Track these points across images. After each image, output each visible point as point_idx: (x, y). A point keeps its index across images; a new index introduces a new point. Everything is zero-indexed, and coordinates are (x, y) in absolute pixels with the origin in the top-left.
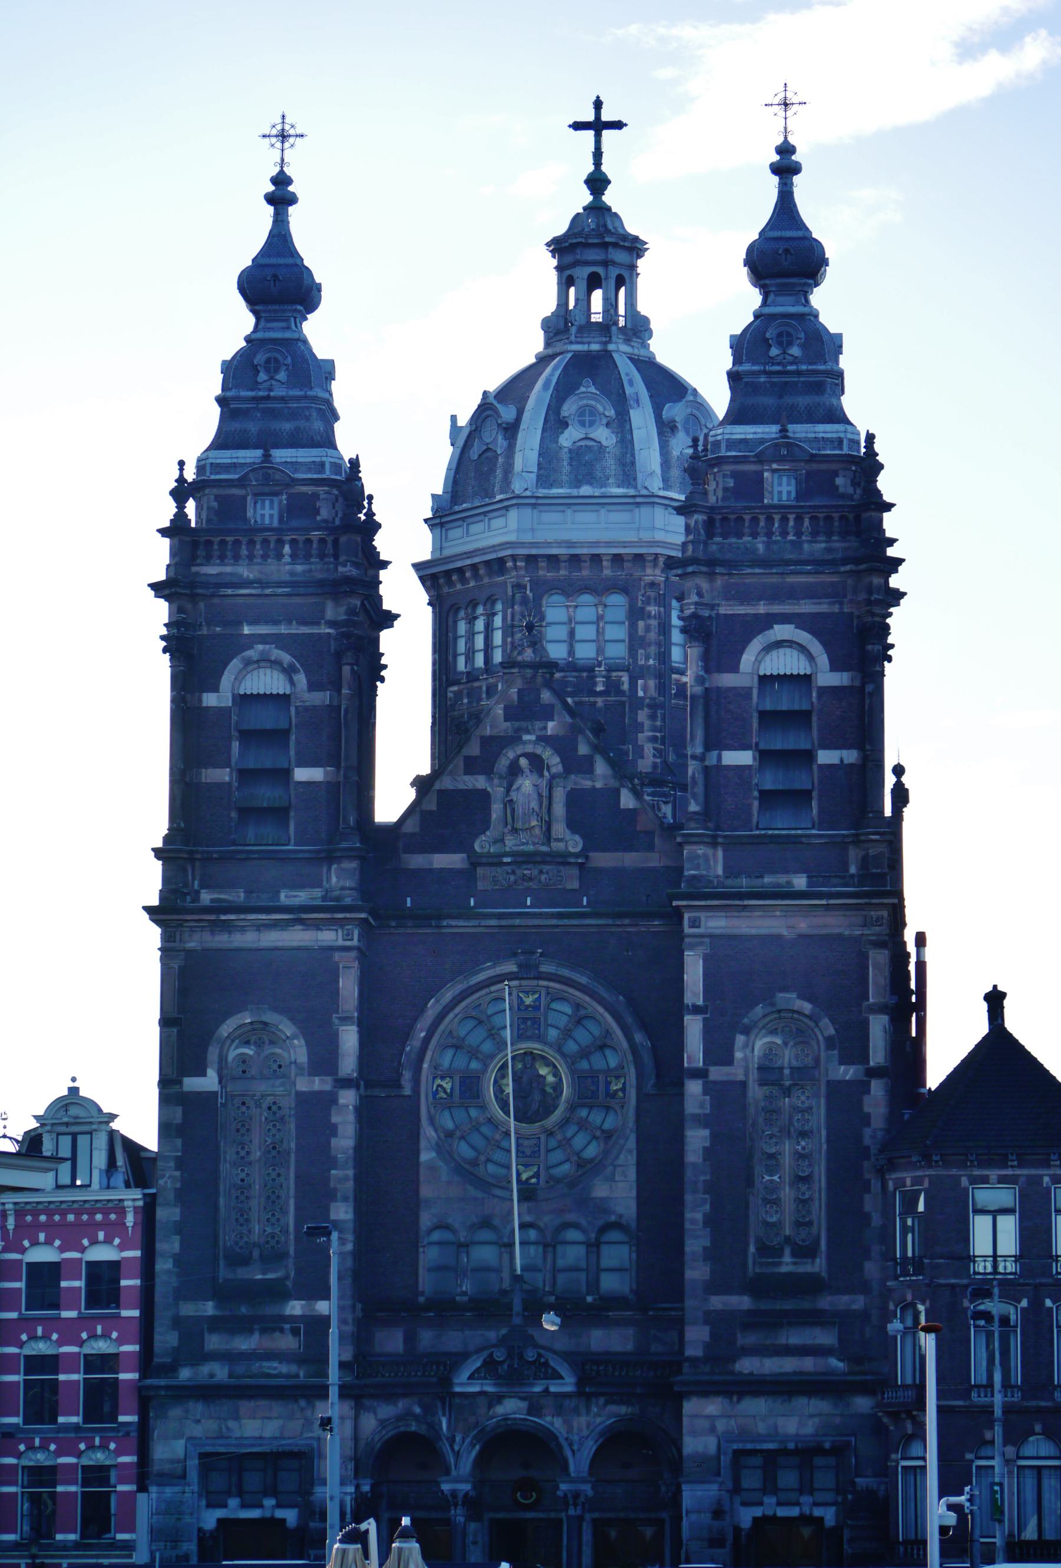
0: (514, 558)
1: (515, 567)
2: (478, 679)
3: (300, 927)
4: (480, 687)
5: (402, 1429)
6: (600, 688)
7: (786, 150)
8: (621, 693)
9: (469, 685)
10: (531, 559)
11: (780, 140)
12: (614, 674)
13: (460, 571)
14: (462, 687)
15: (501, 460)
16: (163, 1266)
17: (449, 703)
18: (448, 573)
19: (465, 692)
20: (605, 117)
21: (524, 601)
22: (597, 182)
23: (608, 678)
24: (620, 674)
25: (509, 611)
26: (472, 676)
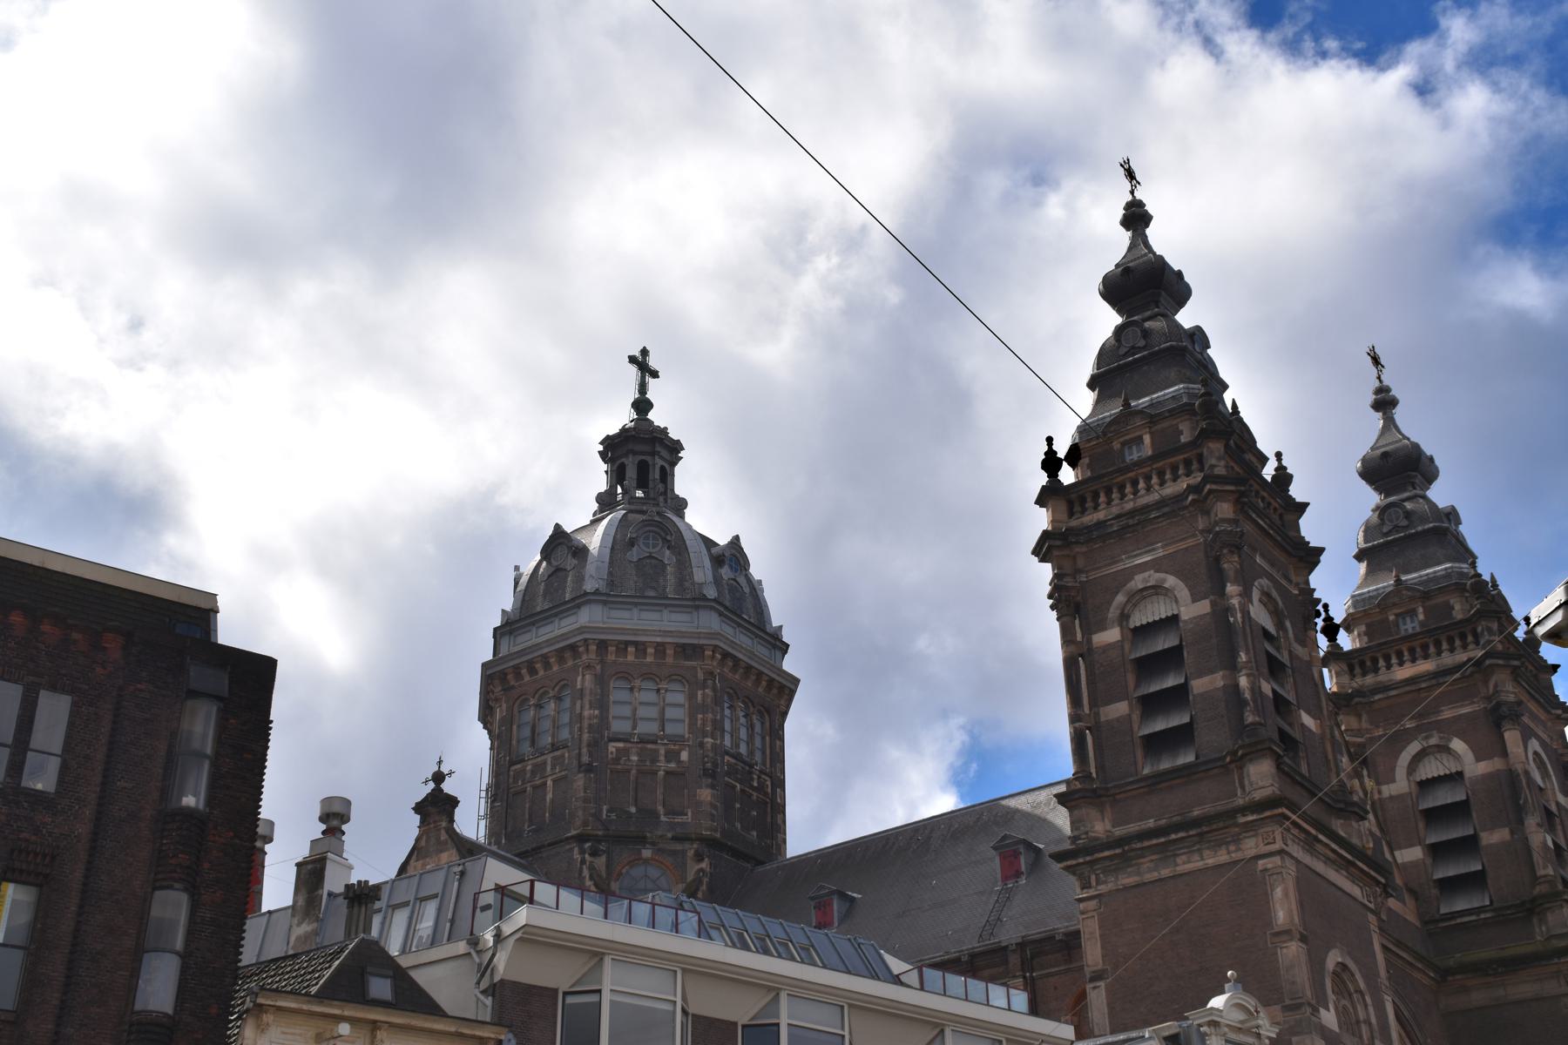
0: (715, 648)
1: (713, 657)
2: (655, 742)
3: (1345, 873)
4: (657, 751)
6: (755, 784)
7: (1382, 390)
8: (766, 794)
9: (640, 746)
10: (726, 655)
11: (1377, 384)
12: (763, 776)
13: (641, 648)
14: (630, 745)
17: (610, 756)
18: (622, 647)
20: (653, 362)
21: (714, 689)
22: (642, 405)
23: (759, 777)
24: (767, 778)
25: (700, 692)
26: (642, 741)
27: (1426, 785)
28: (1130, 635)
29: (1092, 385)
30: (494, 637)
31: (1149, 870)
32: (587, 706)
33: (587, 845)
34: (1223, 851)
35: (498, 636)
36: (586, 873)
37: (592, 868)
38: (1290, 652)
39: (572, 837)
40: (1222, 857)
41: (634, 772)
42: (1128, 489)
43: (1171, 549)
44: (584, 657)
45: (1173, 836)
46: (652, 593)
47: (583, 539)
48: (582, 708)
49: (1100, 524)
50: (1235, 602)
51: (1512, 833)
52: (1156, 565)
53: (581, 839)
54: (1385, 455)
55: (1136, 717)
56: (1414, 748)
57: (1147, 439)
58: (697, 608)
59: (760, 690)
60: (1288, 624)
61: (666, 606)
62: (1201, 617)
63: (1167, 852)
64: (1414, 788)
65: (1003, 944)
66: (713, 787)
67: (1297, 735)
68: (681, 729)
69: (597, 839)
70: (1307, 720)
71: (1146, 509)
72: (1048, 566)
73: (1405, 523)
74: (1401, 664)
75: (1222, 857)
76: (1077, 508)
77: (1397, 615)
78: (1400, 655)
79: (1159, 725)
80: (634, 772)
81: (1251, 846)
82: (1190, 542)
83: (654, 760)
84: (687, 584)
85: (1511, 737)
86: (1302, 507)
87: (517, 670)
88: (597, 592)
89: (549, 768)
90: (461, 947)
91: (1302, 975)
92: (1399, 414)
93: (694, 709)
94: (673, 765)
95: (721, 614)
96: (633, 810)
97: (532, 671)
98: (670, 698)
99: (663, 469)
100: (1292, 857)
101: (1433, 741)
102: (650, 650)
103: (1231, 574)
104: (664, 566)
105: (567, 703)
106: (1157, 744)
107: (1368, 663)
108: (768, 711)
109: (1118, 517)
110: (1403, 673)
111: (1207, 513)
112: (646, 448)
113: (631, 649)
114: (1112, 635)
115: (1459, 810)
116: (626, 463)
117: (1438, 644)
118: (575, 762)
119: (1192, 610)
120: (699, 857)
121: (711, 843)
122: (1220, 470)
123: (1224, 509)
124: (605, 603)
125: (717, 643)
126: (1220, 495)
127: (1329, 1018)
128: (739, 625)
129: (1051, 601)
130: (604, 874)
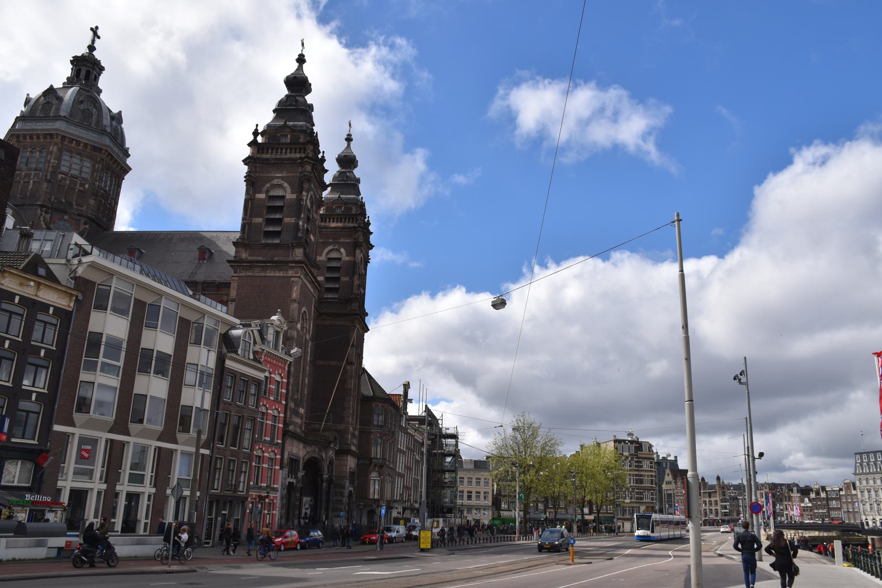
0: (106, 151)
1: (105, 154)
2: (77, 178)
4: (77, 182)
5: (313, 455)
6: (109, 202)
7: (349, 135)
8: (112, 206)
10: (109, 154)
11: (348, 133)
12: (112, 200)
13: (78, 143)
15: (94, 116)
16: (290, 388)
19: (68, 179)
21: (102, 165)
25: (97, 165)
26: (73, 176)
27: (330, 259)
28: (268, 197)
29: (274, 111)
30: (16, 119)
31: (257, 273)
32: (53, 158)
33: (44, 209)
34: (282, 272)
35: (17, 120)
36: (42, 219)
37: (44, 218)
38: (313, 216)
39: (39, 205)
40: (281, 274)
41: (66, 187)
42: (279, 151)
43: (288, 175)
44: (55, 140)
45: (268, 264)
46: (86, 124)
47: (60, 94)
48: (51, 158)
49: (268, 159)
50: (304, 198)
51: (350, 279)
52: (282, 178)
53: (42, 206)
54: (345, 156)
55: (264, 224)
56: (330, 248)
57: (289, 136)
58: (102, 134)
59: (118, 169)
60: (314, 207)
61: (91, 130)
62: (293, 199)
63: (264, 268)
64: (327, 259)
65: (197, 281)
66: (95, 200)
67: (308, 241)
68: (87, 176)
69: (48, 208)
70: (312, 237)
71: (284, 159)
72: (247, 167)
73: (346, 179)
74: (333, 222)
75: (281, 274)
76: (261, 151)
77: (336, 206)
78: (334, 219)
79: (271, 229)
80: (66, 187)
81: (290, 273)
82: (295, 174)
83: (75, 185)
84: (100, 124)
85: (358, 251)
86: (326, 171)
87: (25, 136)
88: (65, 117)
89: (32, 177)
90: (63, 261)
91: (296, 314)
92: (352, 143)
93: (94, 170)
94: (82, 188)
95: (110, 139)
96: (64, 200)
97: (31, 138)
98: (86, 164)
99: (95, 76)
100: (301, 279)
101: (336, 247)
102: (82, 145)
103: (305, 189)
104: (92, 114)
105: (44, 154)
106: (268, 234)
107: (324, 219)
108: (118, 178)
109: (274, 159)
110: (333, 225)
111: (303, 167)
112: (91, 66)
113: (74, 142)
114: (262, 196)
115: (337, 269)
116: (82, 69)
117: (345, 219)
118: (44, 178)
119: (290, 196)
120: (86, 223)
121: (91, 219)
122: (310, 155)
123: (309, 168)
124: (67, 122)
125: (108, 149)
126: (308, 163)
127: (299, 326)
128: (116, 144)
129: (245, 179)
130: (48, 221)
